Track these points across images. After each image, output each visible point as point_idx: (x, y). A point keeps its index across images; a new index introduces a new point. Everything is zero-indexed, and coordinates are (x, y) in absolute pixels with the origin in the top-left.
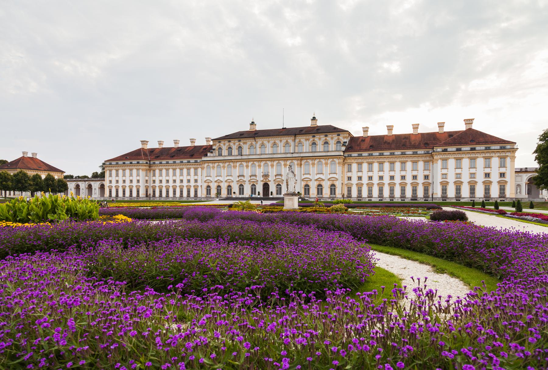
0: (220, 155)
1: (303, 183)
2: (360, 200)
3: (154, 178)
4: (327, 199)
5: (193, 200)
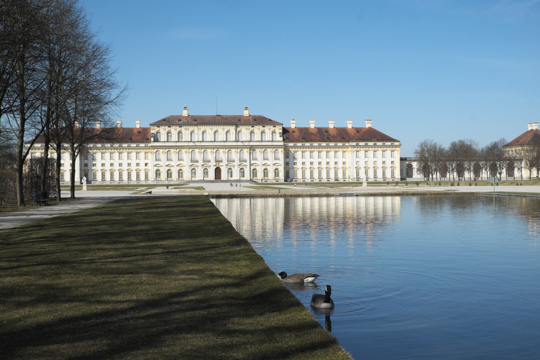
0: (156, 140)
1: (252, 168)
2: (296, 181)
3: (86, 162)
4: (273, 181)
5: (135, 183)
